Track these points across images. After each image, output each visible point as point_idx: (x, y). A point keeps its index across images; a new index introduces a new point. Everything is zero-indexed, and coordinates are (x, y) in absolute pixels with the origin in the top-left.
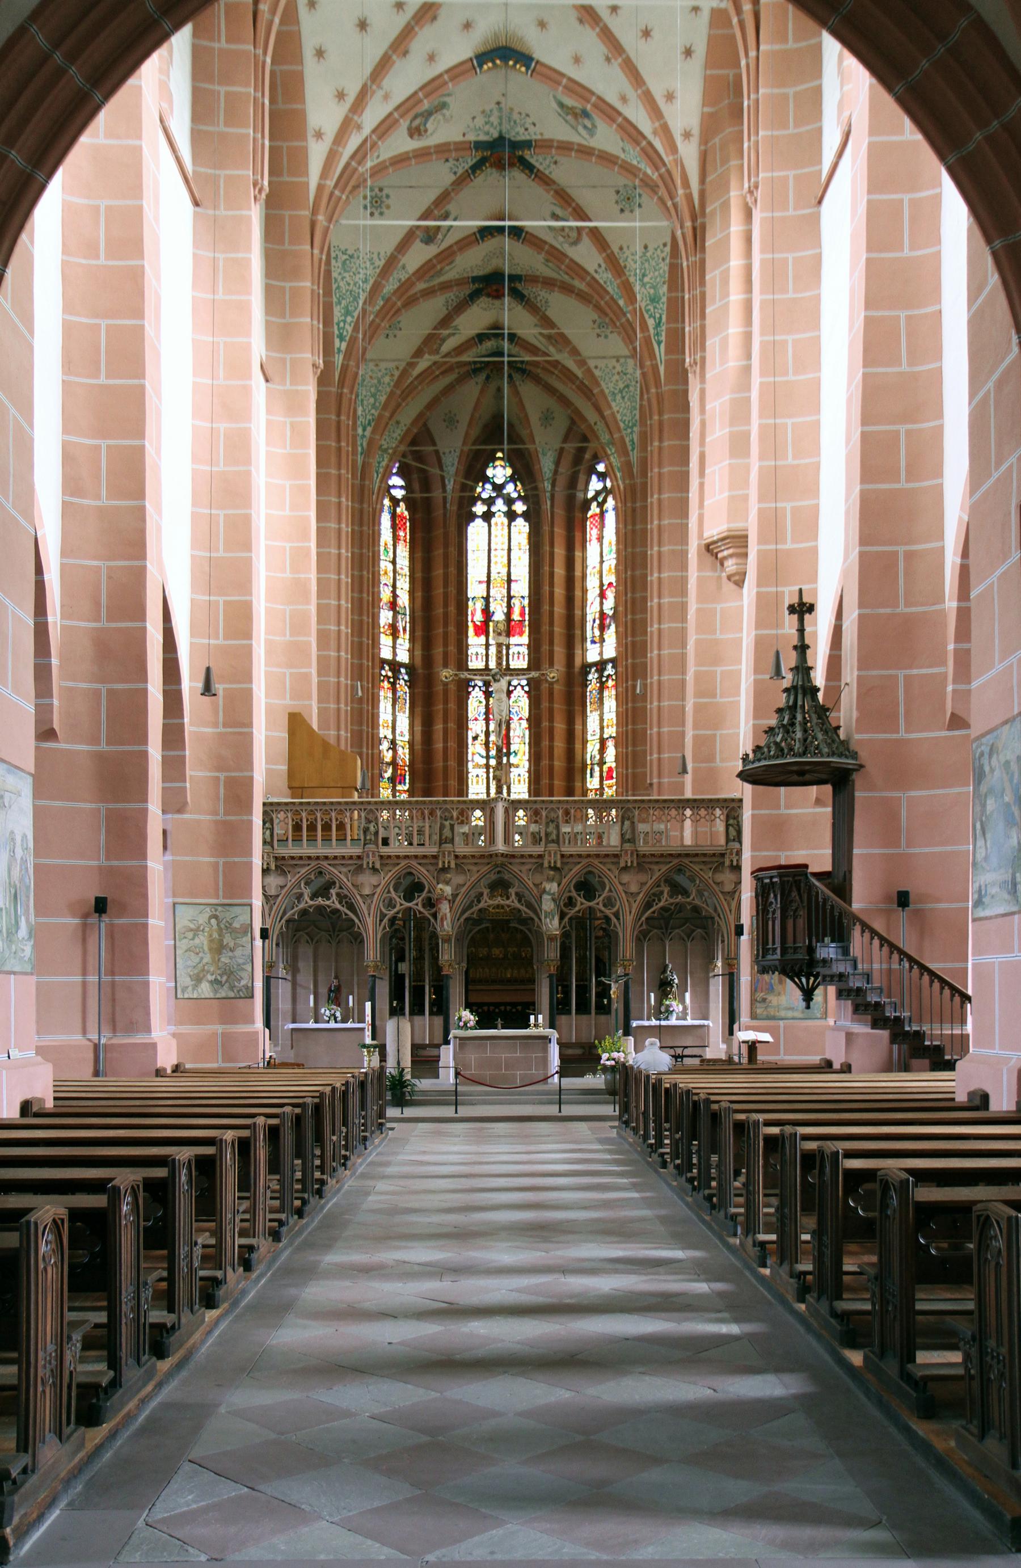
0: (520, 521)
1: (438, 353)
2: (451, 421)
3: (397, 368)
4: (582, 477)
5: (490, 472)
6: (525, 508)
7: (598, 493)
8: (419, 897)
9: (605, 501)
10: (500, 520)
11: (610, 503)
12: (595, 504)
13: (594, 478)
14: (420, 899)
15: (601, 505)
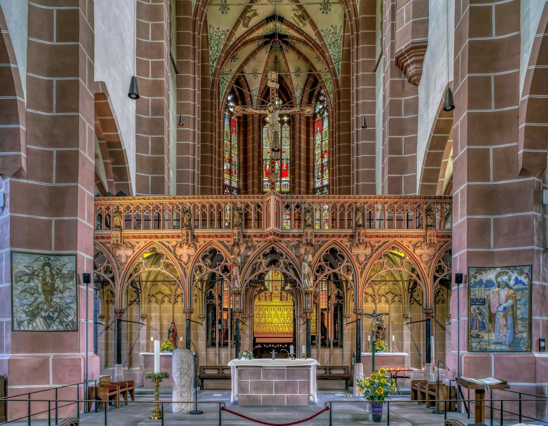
0: (286, 125)
3: (228, 31)
6: (288, 118)
7: (320, 110)
9: (323, 113)
15: (321, 115)
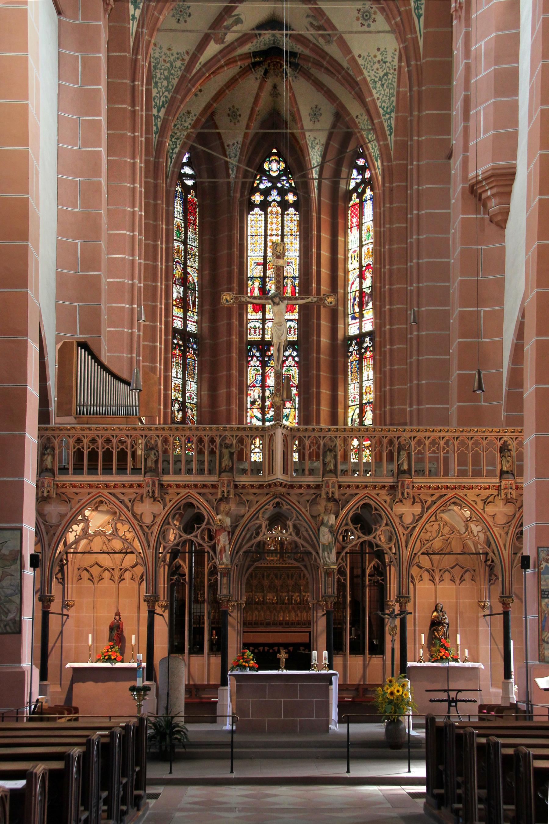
0: (291, 210)
1: (223, 42)
2: (234, 115)
4: (344, 170)
5: (266, 166)
7: (358, 185)
8: (199, 528)
9: (364, 192)
10: (274, 209)
11: (369, 193)
12: (355, 195)
13: (355, 172)
14: (199, 531)
15: (360, 196)
